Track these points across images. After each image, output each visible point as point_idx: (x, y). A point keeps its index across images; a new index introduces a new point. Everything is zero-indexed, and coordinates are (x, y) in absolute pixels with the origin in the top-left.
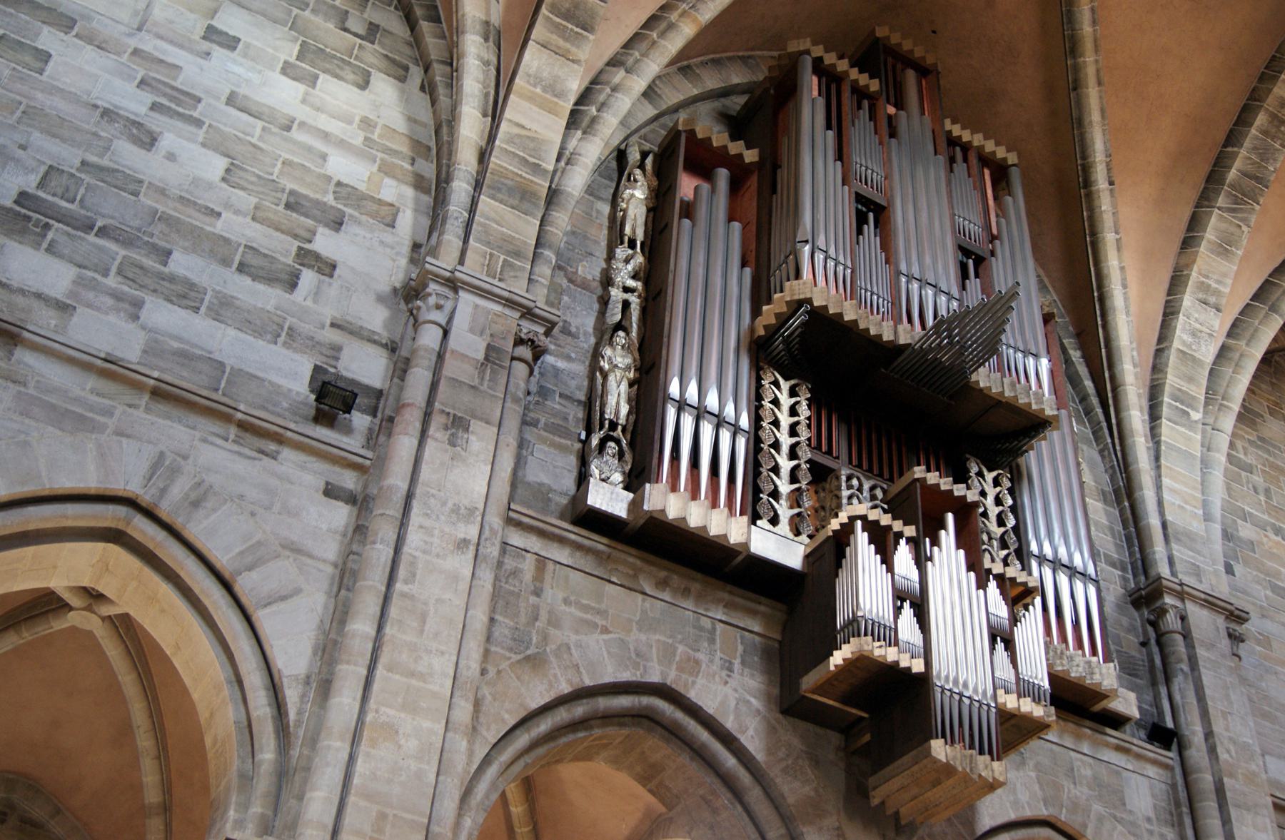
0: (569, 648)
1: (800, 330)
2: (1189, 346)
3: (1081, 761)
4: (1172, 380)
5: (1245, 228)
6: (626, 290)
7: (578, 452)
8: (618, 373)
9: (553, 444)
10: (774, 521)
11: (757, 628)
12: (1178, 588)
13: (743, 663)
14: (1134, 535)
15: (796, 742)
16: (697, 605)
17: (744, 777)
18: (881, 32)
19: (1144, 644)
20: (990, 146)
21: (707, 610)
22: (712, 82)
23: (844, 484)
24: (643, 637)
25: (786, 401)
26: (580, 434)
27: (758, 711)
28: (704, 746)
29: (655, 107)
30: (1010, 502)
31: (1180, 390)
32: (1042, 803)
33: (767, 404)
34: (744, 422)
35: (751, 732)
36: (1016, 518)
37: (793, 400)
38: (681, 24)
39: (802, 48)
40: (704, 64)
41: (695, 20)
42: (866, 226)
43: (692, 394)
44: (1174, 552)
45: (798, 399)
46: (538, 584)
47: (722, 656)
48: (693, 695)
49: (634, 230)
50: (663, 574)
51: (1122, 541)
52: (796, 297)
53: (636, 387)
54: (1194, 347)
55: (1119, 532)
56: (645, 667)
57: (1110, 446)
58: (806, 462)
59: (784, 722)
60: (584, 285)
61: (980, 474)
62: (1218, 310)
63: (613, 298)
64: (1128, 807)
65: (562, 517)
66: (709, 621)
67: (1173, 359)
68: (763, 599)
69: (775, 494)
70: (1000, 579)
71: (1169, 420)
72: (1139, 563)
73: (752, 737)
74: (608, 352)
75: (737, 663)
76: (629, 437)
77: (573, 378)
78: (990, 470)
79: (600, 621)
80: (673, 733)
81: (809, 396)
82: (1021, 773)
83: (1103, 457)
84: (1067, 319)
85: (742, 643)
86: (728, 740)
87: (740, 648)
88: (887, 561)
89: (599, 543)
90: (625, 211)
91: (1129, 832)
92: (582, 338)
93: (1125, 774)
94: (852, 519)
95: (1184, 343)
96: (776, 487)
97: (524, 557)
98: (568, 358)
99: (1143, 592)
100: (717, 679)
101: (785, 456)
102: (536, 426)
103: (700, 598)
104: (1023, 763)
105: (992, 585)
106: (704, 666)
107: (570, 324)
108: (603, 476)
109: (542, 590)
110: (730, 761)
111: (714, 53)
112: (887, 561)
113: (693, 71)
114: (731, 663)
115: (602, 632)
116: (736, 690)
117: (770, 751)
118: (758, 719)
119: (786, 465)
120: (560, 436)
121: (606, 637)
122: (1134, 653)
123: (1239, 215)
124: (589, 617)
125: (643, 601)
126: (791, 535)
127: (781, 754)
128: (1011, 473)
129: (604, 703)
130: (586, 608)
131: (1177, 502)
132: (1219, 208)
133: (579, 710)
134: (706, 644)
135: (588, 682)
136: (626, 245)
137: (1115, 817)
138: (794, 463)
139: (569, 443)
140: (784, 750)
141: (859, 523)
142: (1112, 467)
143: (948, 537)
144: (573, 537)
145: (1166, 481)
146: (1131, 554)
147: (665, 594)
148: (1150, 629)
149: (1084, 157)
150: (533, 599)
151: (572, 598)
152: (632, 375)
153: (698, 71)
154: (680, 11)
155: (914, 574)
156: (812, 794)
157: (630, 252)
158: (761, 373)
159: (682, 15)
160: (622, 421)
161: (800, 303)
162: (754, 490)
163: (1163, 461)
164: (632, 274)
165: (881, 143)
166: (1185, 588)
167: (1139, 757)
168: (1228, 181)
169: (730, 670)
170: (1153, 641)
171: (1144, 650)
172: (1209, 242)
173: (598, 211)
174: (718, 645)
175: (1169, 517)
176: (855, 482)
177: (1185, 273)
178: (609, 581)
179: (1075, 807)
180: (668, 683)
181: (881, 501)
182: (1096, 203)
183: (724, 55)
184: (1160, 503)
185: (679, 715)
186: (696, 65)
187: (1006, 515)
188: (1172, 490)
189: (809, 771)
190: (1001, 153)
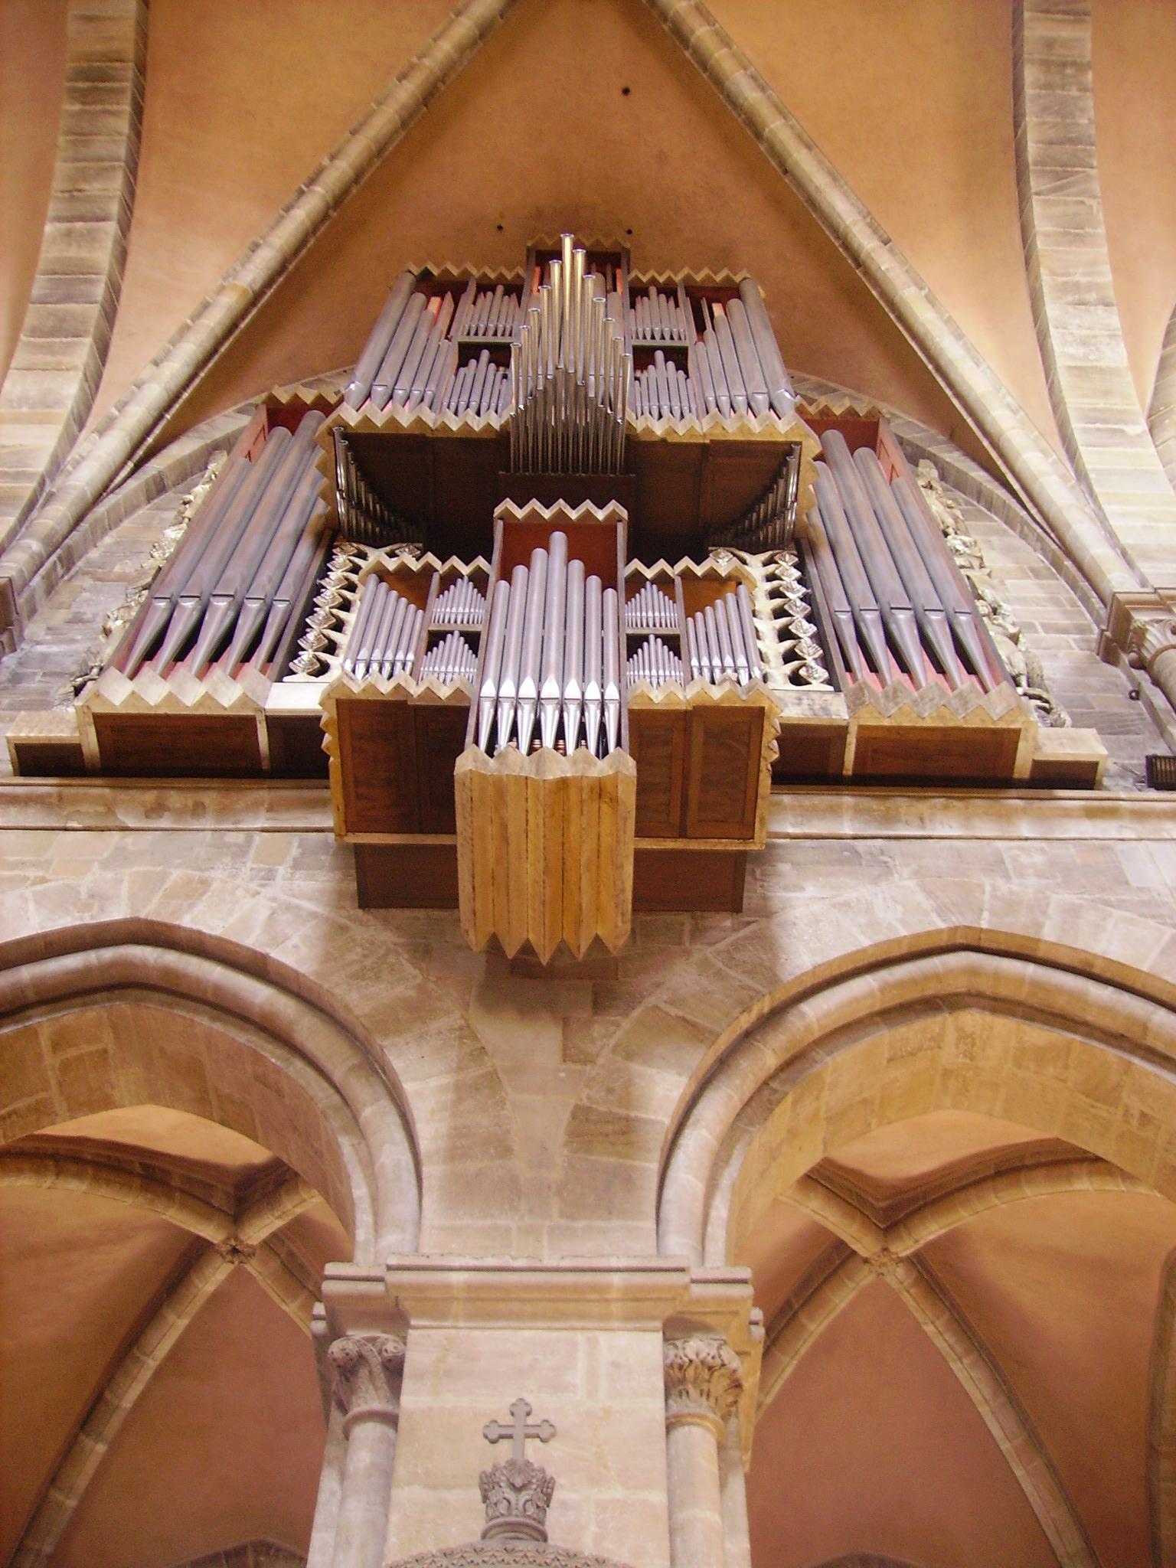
2: (1086, 358)
4: (1073, 403)
5: (1089, 201)
11: (329, 822)
12: (1153, 597)
15: (386, 937)
16: (219, 821)
17: (285, 1007)
19: (1136, 695)
24: (109, 875)
28: (218, 989)
31: (1094, 410)
32: (934, 916)
35: (295, 940)
47: (254, 866)
50: (150, 796)
54: (1092, 357)
62: (1107, 304)
64: (1134, 884)
67: (1063, 379)
73: (295, 947)
75: (282, 871)
82: (884, 885)
86: (257, 967)
91: (1141, 915)
93: (1120, 845)
95: (1073, 357)
103: (223, 812)
110: (257, 993)
122: (1125, 711)
123: (1071, 190)
127: (352, 957)
132: (1038, 194)
142: (1039, 539)
156: (412, 993)
166: (1160, 591)
167: (1140, 815)
168: (1030, 160)
171: (1140, 702)
172: (1046, 235)
175: (1125, 540)
178: (66, 829)
179: (1011, 905)
180: (142, 915)
182: (873, 268)
184: (1112, 537)
185: (172, 959)
189: (410, 969)
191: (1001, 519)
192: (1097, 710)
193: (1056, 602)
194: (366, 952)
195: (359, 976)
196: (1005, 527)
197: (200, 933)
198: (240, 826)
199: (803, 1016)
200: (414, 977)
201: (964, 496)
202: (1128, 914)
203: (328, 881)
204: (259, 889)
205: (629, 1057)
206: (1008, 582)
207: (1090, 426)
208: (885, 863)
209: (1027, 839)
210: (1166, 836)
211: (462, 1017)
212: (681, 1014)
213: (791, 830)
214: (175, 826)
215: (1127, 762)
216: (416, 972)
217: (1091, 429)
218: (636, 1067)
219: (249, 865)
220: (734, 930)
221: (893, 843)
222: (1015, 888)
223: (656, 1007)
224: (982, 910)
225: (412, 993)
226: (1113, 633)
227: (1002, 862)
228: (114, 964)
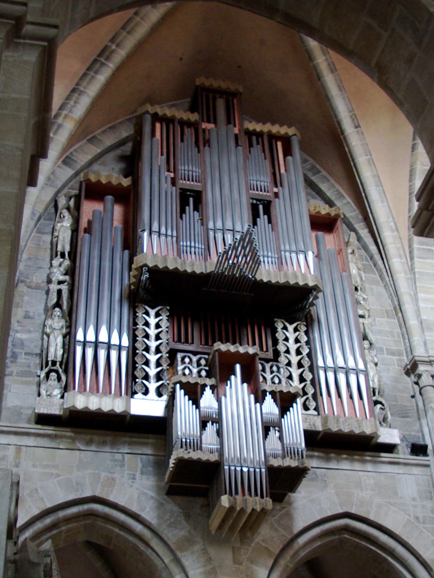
0: (37, 490)
1: (148, 282)
6: (60, 283)
7: (37, 383)
8: (56, 332)
9: (22, 383)
10: (146, 392)
11: (149, 452)
12: (427, 359)
13: (142, 473)
14: (405, 333)
15: (176, 509)
16: (112, 448)
18: (198, 82)
19: (413, 397)
20: (275, 129)
21: (118, 449)
22: (109, 141)
23: (179, 363)
25: (153, 321)
26: (37, 373)
27: (152, 497)
29: (73, 169)
30: (306, 339)
32: (339, 506)
33: (140, 326)
34: (125, 342)
35: (148, 509)
36: (310, 349)
37: (157, 320)
38: (64, 123)
39: (143, 111)
40: (104, 132)
41: (72, 118)
42: (187, 208)
43: (91, 337)
44: (427, 338)
45: (161, 318)
46: (17, 461)
47: (129, 472)
48: (112, 498)
49: (63, 247)
50: (88, 437)
51: (399, 337)
52: (139, 265)
53: (68, 337)
55: (398, 333)
56: (82, 490)
57: (388, 282)
58: (167, 353)
59: (168, 499)
60: (38, 288)
61: (285, 328)
63: (51, 291)
65: (29, 422)
66: (120, 455)
68: (150, 436)
69: (147, 377)
70: (273, 393)
71: (420, 258)
72: (409, 349)
73: (149, 512)
74: (49, 322)
75: (138, 474)
76: (63, 367)
77: (32, 342)
78: (291, 323)
79: (54, 471)
80: (107, 518)
81: (168, 314)
83: (386, 289)
84: (358, 212)
85: (141, 462)
87: (140, 465)
88: (196, 403)
89: (49, 430)
90: (57, 237)
92: (37, 318)
93: (398, 476)
94: (175, 384)
97: (8, 449)
98: (29, 332)
99: (409, 367)
101: (153, 354)
102: (11, 375)
103: (113, 444)
104: (326, 486)
105: (269, 398)
106: (117, 481)
107: (29, 312)
108: (48, 393)
109: (19, 463)
110: (138, 527)
111: (108, 123)
112: (196, 403)
113: (97, 138)
114: (134, 475)
115: (55, 477)
116: (138, 489)
117: (159, 517)
118: (152, 501)
119: (153, 358)
120: (26, 377)
121: (59, 479)
124: (48, 471)
125: (80, 454)
126: (157, 398)
127: (167, 517)
128: (306, 322)
129: (61, 514)
130: (47, 466)
131: (429, 306)
133: (48, 521)
134: (118, 468)
135: (49, 505)
136: (59, 256)
137: (390, 503)
138: (159, 356)
139: (31, 379)
140: (168, 514)
141: (178, 386)
142: (391, 294)
143: (236, 380)
144: (33, 431)
145: (421, 295)
146: (405, 344)
147: (92, 447)
148: (416, 387)
149: (336, 117)
151: (38, 463)
152: (64, 331)
153: (100, 138)
154: (63, 116)
155: (215, 405)
156: (187, 534)
157: (62, 260)
158: (137, 310)
159: (66, 116)
160: (59, 359)
161: (142, 267)
162: (132, 377)
163: (417, 284)
164: (64, 272)
165: (199, 152)
169: (134, 478)
170: (418, 394)
171: (414, 400)
173: (44, 241)
174: (126, 467)
176: (187, 360)
177: (415, 166)
178: (59, 449)
180: (97, 494)
181: (205, 366)
183: (117, 122)
186: (99, 134)
187: (302, 348)
188: (426, 300)
189: (184, 522)
190: (283, 130)
191: (379, 274)
192: (399, 403)
193: (391, 333)
195: (169, 526)
196: (379, 279)
197: (117, 503)
198: (120, 451)
199: (298, 543)
200: (187, 527)
201: (365, 254)
203: (152, 481)
204: (132, 484)
205: (252, 562)
206: (377, 319)
207: (421, 247)
208: (326, 481)
209: (369, 471)
210: (412, 473)
211: (203, 545)
214: (97, 450)
215: (405, 433)
216: (187, 525)
217: (420, 248)
218: (254, 567)
219: (127, 472)
220: (281, 510)
221: (328, 470)
223: (258, 542)
224: (353, 505)
226: (411, 367)
227: (360, 482)
228: (88, 510)
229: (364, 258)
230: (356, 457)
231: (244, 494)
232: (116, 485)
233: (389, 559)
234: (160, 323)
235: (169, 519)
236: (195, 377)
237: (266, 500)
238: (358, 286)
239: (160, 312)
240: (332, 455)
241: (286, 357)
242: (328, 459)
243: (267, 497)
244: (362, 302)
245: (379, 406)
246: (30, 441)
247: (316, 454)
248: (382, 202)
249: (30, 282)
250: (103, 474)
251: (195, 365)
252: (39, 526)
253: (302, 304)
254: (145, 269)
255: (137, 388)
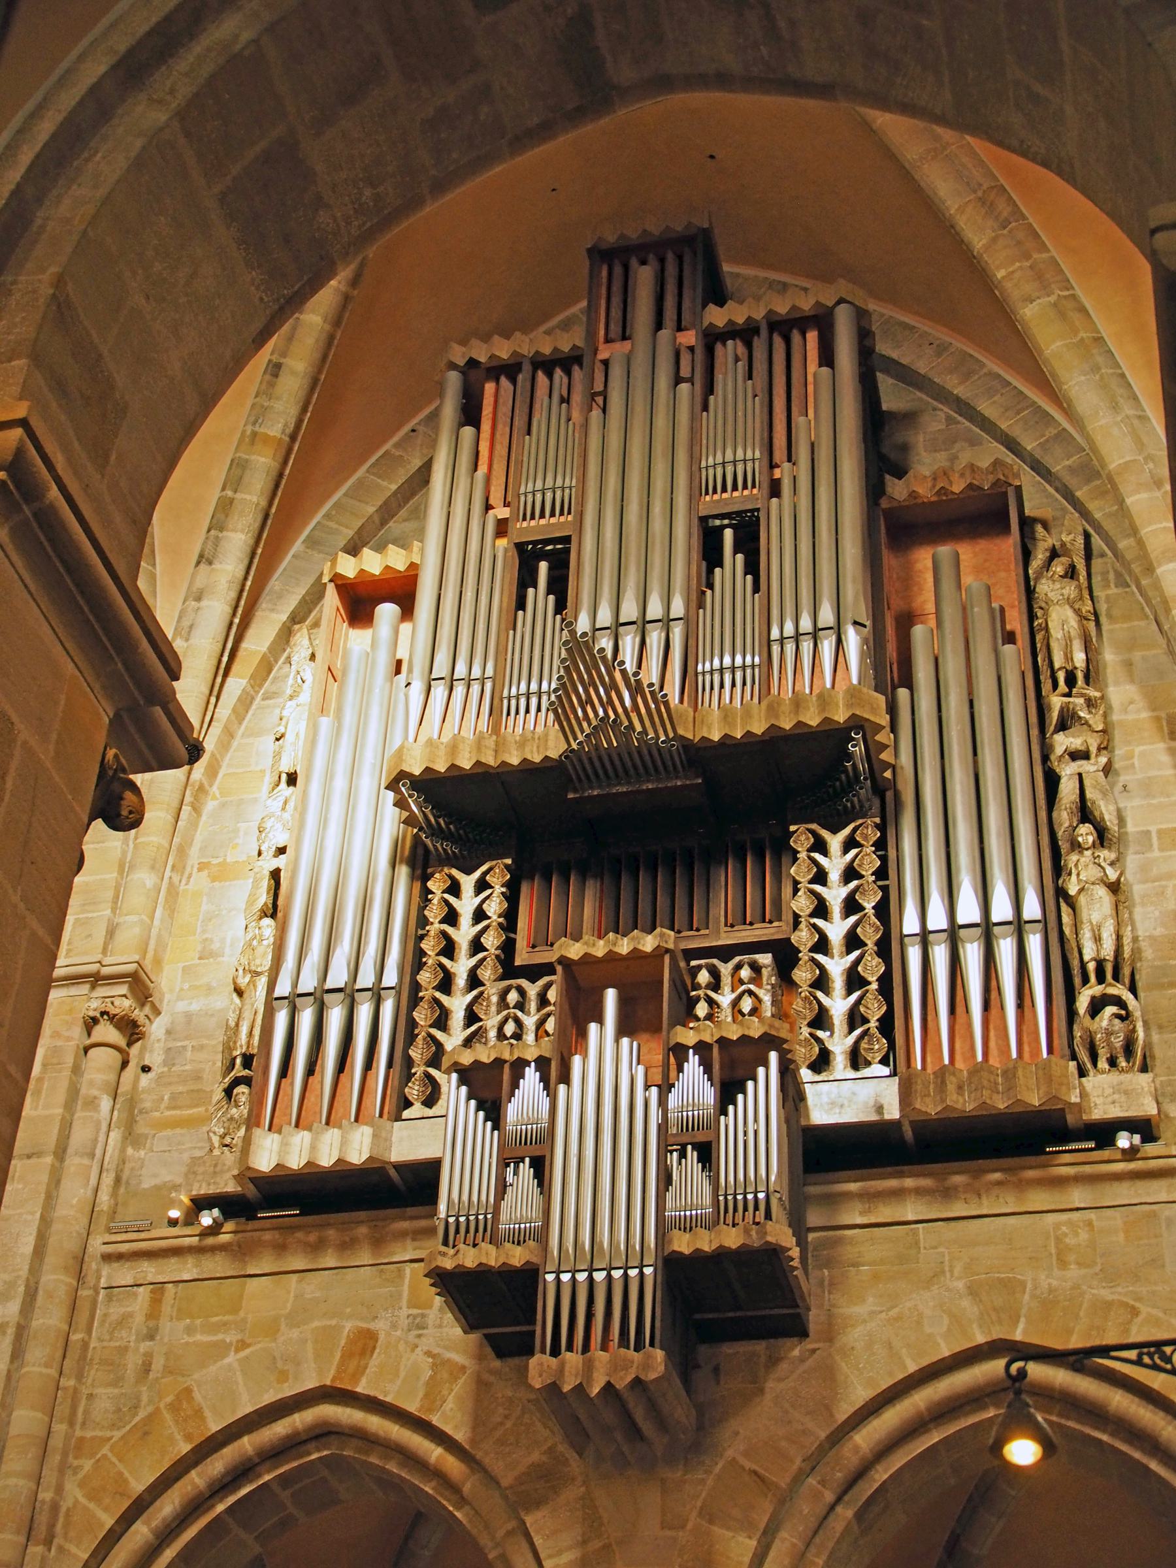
3: (1070, 1223)
46: (151, 1324)
50: (312, 1237)
70: (702, 1048)
78: (835, 831)
88: (493, 1111)
96: (439, 1046)
97: (135, 1295)
100: (401, 1346)
101: (459, 993)
103: (378, 1242)
106: (382, 1336)
107: (212, 940)
109: (157, 1329)
112: (493, 1111)
115: (237, 1351)
116: (428, 1353)
121: (242, 1354)
125: (300, 1281)
133: (217, 1465)
150: (145, 1346)
156: (544, 1458)
162: (402, 1066)
176: (513, 997)
194: (507, 1412)
202: (1154, 1312)
204: (416, 1341)
209: (1078, 1209)
212: (755, 1467)
213: (859, 1220)
222: (1055, 1283)
225: (544, 1458)
229: (1111, 576)
230: (1030, 1174)
231: (586, 1348)
232: (377, 1351)
233: (1154, 1465)
234: (485, 906)
235: (502, 1424)
236: (494, 1046)
237: (649, 1356)
238: (1076, 668)
239: (488, 878)
240: (958, 1179)
241: (814, 926)
242: (947, 1194)
243: (652, 1344)
244: (1082, 714)
245: (1110, 1010)
246: (187, 1269)
247: (909, 1182)
248: (1115, 407)
249: (219, 864)
250: (348, 1326)
251: (533, 1006)
252: (197, 1479)
253: (846, 771)
254: (404, 785)
255: (414, 1091)
